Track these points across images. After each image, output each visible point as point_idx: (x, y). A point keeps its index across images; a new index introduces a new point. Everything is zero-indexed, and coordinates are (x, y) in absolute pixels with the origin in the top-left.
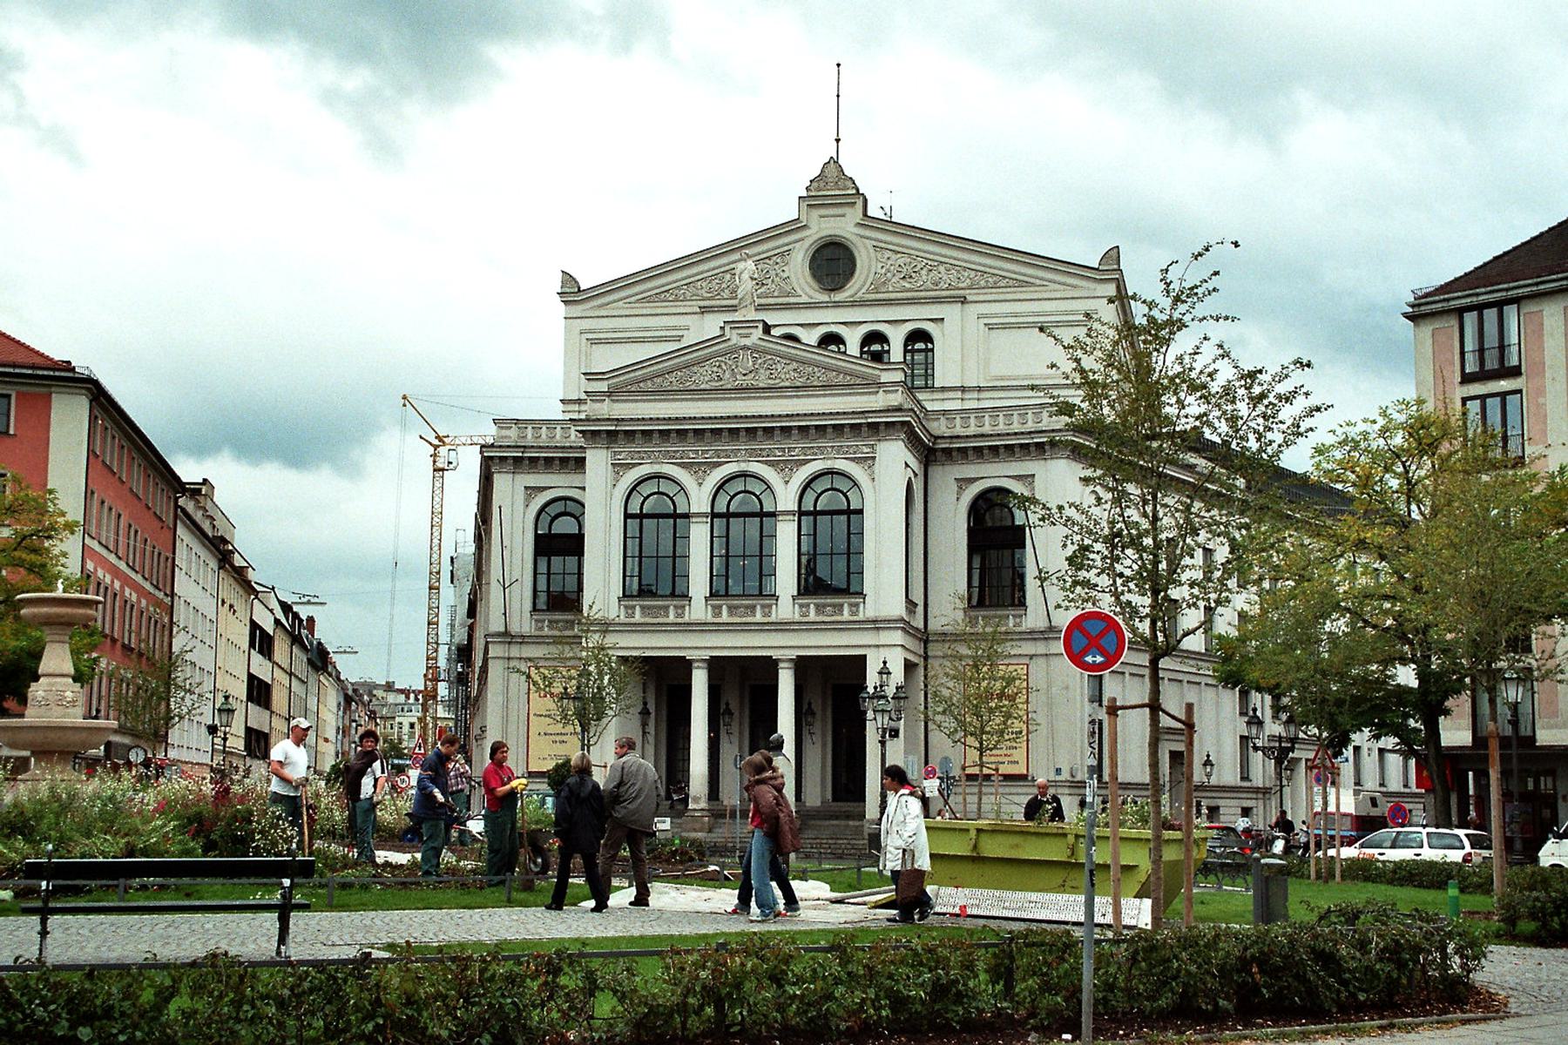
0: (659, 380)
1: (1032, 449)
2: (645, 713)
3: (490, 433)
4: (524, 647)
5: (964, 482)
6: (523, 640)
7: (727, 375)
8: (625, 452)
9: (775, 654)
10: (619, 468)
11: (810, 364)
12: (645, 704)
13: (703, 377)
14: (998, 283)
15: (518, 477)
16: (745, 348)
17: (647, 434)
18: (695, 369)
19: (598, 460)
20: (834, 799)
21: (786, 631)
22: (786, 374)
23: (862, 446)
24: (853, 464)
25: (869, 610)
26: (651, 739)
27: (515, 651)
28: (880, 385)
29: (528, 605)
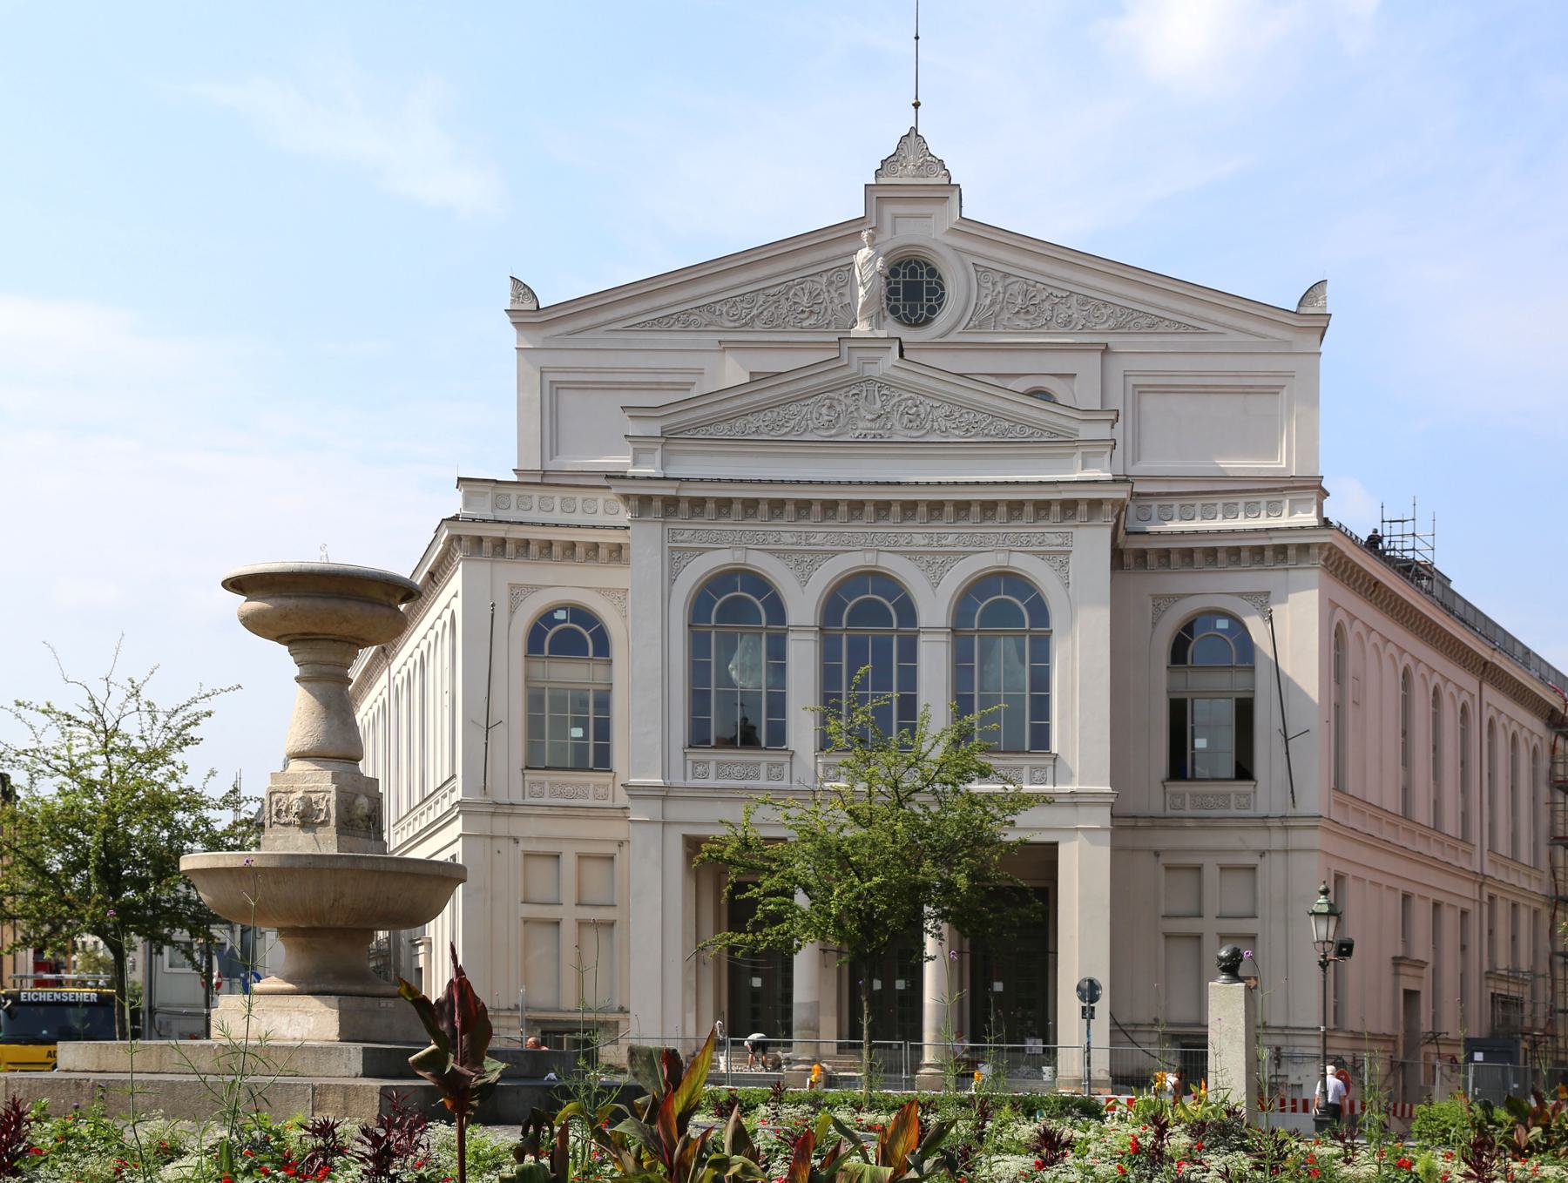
0: (740, 423)
1: (1269, 554)
8: (688, 529)
10: (675, 559)
11: (969, 410)
14: (1154, 325)
18: (794, 408)
19: (647, 541)
23: (1051, 533)
24: (1037, 560)
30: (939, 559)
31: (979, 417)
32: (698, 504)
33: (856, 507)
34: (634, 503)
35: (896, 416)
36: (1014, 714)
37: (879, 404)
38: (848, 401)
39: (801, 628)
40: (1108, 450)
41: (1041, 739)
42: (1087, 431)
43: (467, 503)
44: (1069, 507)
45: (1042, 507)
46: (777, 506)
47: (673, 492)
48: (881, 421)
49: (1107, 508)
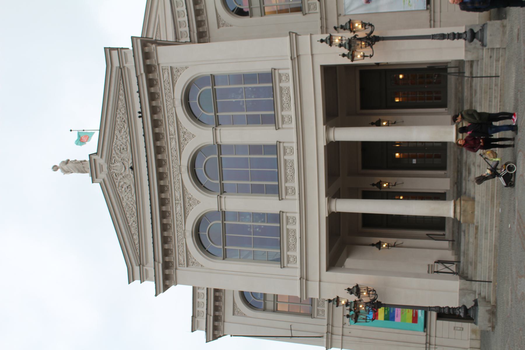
0: (132, 229)
2: (379, 245)
3: (201, 334)
4: (335, 324)
5: (219, 23)
6: (330, 325)
7: (126, 180)
8: (179, 257)
9: (323, 143)
12: (373, 245)
13: (128, 198)
15: (227, 319)
16: (109, 168)
17: (165, 240)
18: (124, 204)
20: (444, 106)
21: (304, 136)
22: (122, 138)
23: (164, 78)
25: (285, 66)
26: (399, 241)
27: (338, 330)
28: (121, 68)
29: (308, 320)
30: (181, 134)
31: (118, 116)
32: (166, 253)
33: (161, 176)
34: (167, 283)
35: (122, 156)
36: (256, 92)
37: (118, 164)
38: (119, 179)
39: (220, 204)
40: (123, 51)
41: (268, 77)
42: (116, 64)
43: (201, 329)
44: (149, 69)
45: (151, 83)
46: (164, 215)
47: (160, 265)
48: (125, 163)
49: (147, 49)
